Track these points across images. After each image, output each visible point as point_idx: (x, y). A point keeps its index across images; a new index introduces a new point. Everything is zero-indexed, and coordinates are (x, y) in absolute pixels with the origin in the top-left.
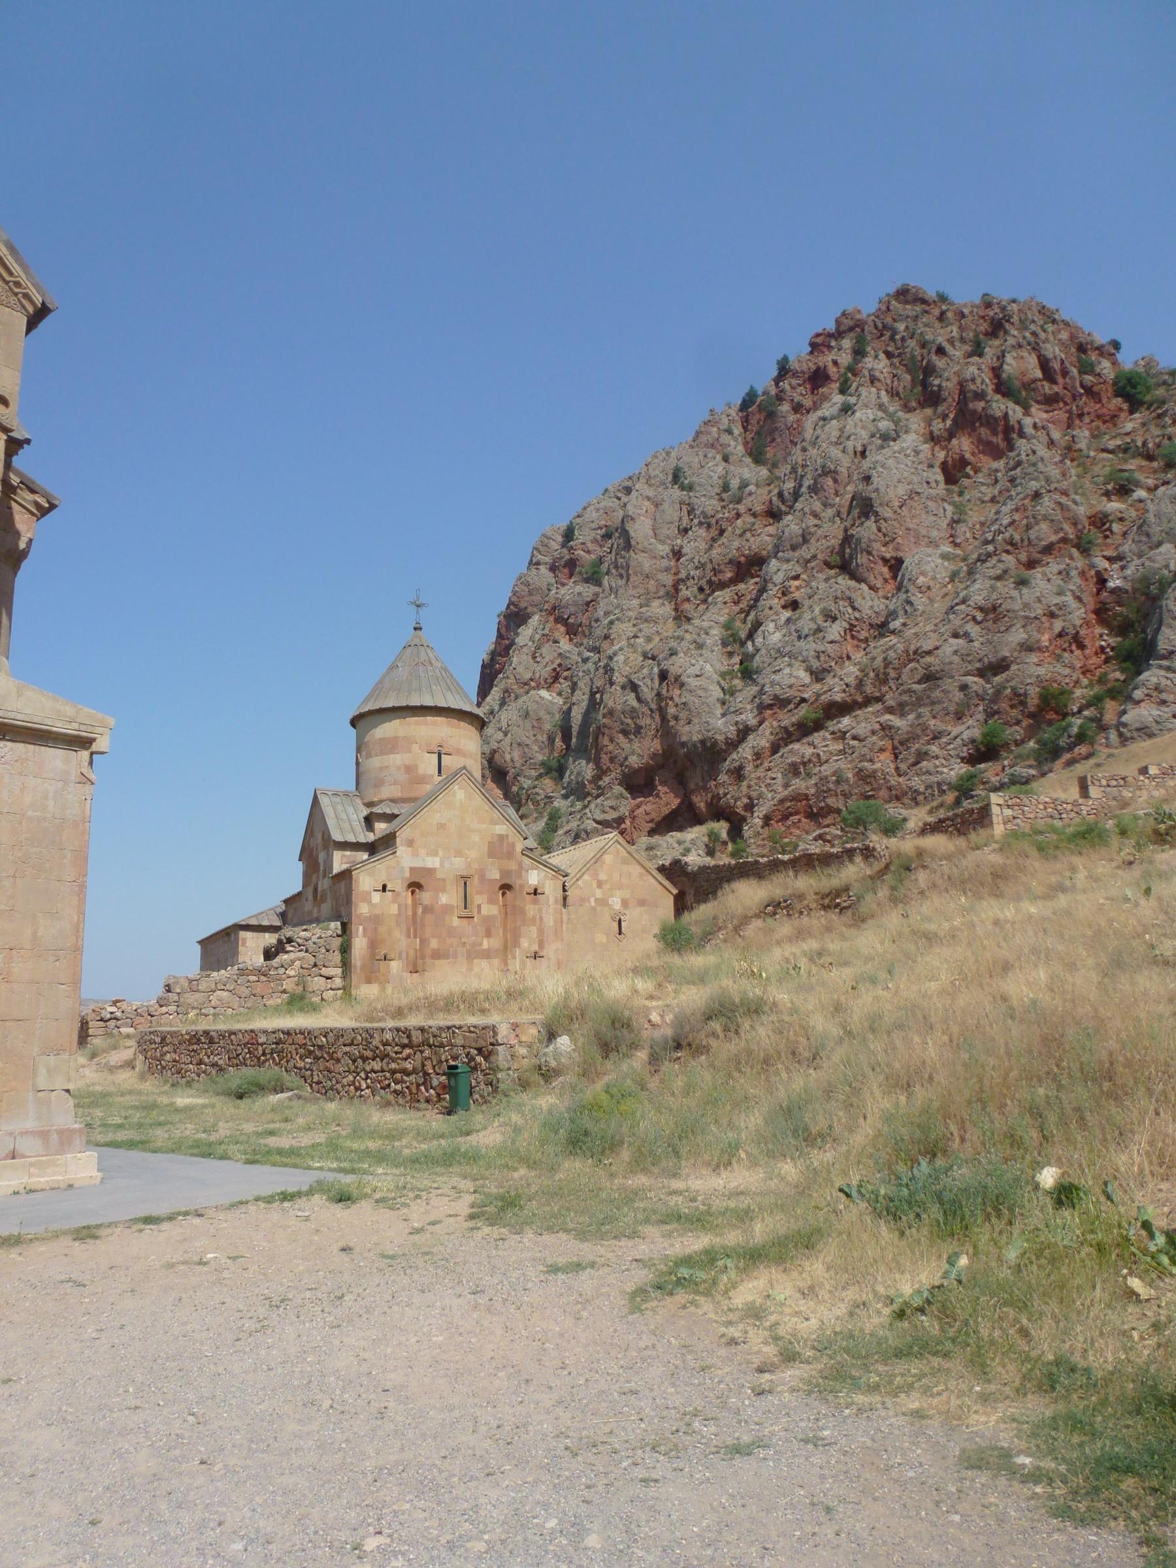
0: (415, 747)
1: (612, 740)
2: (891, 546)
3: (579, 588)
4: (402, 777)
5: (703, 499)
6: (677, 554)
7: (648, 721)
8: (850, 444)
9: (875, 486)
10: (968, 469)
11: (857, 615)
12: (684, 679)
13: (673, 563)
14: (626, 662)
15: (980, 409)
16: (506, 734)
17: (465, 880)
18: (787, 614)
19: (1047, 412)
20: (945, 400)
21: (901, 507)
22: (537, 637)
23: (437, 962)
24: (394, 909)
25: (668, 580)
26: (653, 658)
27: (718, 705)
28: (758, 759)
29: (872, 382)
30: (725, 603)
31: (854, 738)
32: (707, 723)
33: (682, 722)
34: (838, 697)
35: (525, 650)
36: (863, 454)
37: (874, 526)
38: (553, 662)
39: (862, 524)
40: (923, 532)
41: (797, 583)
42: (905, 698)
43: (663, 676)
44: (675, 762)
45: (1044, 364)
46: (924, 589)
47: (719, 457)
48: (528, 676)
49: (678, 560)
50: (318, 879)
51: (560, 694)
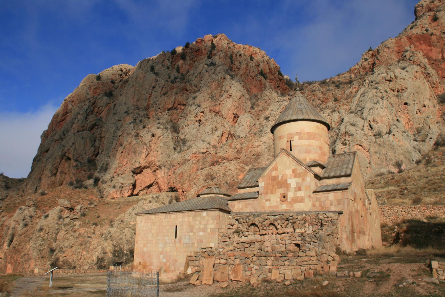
0: (322, 139)
2: (236, 110)
4: (319, 151)
7: (145, 151)
8: (220, 75)
9: (232, 90)
10: (249, 93)
11: (225, 129)
12: (161, 138)
13: (148, 98)
15: (253, 76)
16: (73, 144)
18: (197, 124)
19: (270, 83)
21: (240, 98)
22: (88, 111)
23: (360, 235)
27: (173, 149)
28: (190, 171)
29: (220, 58)
31: (230, 170)
33: (159, 153)
34: (223, 156)
35: (84, 115)
36: (225, 78)
37: (231, 103)
38: (92, 122)
40: (244, 108)
41: (202, 114)
42: (248, 160)
43: (153, 136)
46: (249, 126)
47: (166, 67)
49: (150, 96)
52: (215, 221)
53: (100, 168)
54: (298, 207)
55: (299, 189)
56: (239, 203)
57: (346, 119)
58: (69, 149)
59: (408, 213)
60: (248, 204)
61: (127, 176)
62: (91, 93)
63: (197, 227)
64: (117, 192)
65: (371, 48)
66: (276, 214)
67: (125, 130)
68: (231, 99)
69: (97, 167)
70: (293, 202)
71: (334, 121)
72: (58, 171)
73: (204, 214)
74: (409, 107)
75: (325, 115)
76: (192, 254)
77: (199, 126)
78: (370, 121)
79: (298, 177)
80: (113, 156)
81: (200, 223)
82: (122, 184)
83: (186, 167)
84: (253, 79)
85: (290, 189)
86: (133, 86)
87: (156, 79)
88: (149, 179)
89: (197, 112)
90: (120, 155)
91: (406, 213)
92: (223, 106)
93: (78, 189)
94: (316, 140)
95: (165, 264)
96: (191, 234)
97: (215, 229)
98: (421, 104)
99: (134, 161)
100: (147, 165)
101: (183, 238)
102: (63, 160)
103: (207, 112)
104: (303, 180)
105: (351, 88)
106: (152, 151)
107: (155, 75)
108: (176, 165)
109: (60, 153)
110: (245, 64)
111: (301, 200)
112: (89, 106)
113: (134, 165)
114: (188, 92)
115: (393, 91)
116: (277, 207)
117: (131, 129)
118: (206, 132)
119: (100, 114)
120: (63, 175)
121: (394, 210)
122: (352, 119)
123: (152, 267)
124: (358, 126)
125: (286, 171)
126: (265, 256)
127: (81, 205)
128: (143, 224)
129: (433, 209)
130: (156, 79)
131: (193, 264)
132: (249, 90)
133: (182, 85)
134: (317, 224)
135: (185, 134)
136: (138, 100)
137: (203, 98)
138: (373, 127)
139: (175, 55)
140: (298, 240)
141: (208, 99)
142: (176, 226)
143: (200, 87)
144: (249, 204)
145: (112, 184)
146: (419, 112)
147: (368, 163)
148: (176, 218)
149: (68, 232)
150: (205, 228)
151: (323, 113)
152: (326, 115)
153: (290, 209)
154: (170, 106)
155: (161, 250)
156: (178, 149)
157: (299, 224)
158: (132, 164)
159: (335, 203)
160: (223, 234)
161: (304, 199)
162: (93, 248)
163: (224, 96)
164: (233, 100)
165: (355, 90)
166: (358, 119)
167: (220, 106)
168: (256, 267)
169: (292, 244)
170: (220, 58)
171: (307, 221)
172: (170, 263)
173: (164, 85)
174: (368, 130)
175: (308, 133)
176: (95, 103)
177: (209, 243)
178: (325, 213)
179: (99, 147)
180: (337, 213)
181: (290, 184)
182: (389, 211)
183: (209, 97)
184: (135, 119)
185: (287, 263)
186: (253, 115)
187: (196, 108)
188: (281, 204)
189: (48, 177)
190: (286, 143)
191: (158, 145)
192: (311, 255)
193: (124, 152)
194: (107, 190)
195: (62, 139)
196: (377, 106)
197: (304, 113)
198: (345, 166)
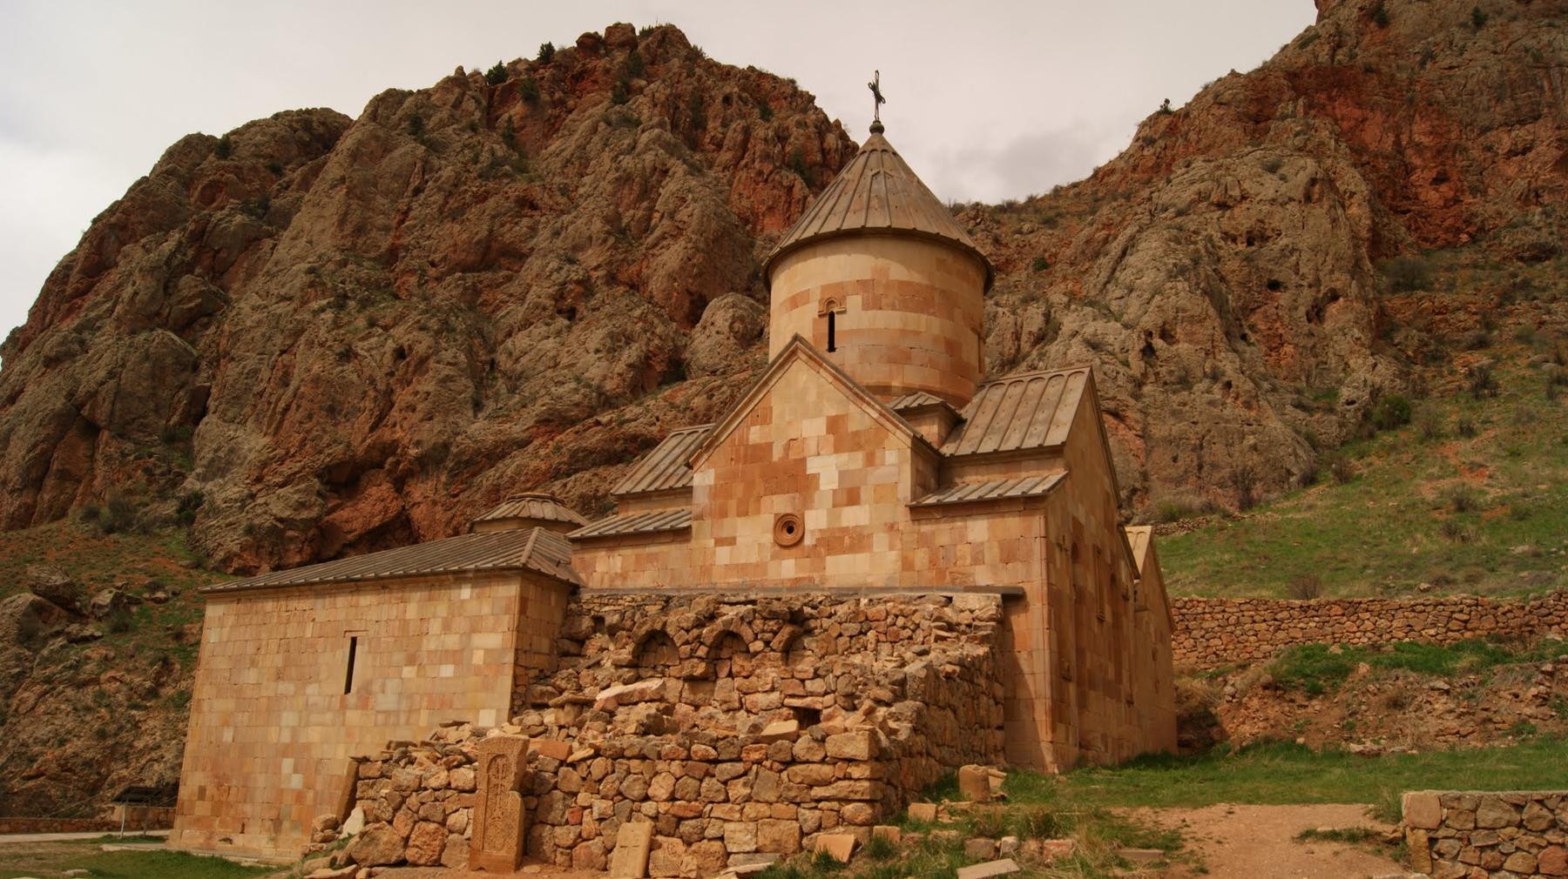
1: (310, 417)
3: (238, 218)
5: (443, 162)
6: (406, 214)
7: (368, 404)
12: (432, 363)
13: (394, 223)
14: (336, 324)
15: (766, 172)
16: (111, 374)
17: (1098, 552)
18: (562, 322)
20: (729, 149)
22: (176, 262)
23: (1092, 694)
24: (1067, 589)
25: (385, 244)
26: (386, 328)
27: (469, 406)
28: (528, 481)
29: (655, 105)
30: (466, 289)
32: (456, 423)
34: (644, 431)
36: (665, 172)
38: (190, 300)
39: (668, 247)
43: (400, 354)
44: (398, 463)
45: (824, 152)
48: (154, 308)
49: (402, 221)
50: (807, 503)
51: (193, 343)
52: (507, 617)
53: (204, 462)
54: (843, 569)
55: (852, 497)
56: (611, 549)
57: (1069, 322)
58: (92, 395)
59: (1278, 629)
60: (649, 555)
61: (297, 492)
62: (192, 200)
63: (432, 646)
64: (258, 547)
65: (1167, 101)
66: (753, 597)
67: (303, 331)
68: (682, 242)
69: (194, 459)
70: (822, 550)
71: (1030, 333)
72: (48, 468)
73: (466, 592)
74: (1283, 298)
75: (1000, 309)
76: (373, 753)
77: (569, 328)
78: (1150, 334)
79: (852, 450)
80: (257, 420)
81: (447, 627)
82: (281, 520)
83: (509, 467)
84: (766, 181)
85: (816, 496)
86: (343, 180)
87: (426, 162)
88: (379, 506)
89: (561, 280)
90: (278, 417)
91: (1271, 629)
92: (653, 265)
93: (115, 536)
94: (933, 314)
95: (299, 797)
96: (409, 672)
97: (504, 650)
98: (1323, 290)
99: (326, 439)
100: (375, 454)
101: (376, 687)
102: (70, 434)
103: (599, 282)
104: (870, 460)
105: (1095, 226)
106: (396, 407)
107: (423, 147)
108: (479, 459)
109: (59, 405)
110: (739, 129)
111: (856, 541)
112: (180, 243)
113: (329, 455)
114: (534, 213)
115: (1234, 240)
116: (760, 567)
117: (323, 329)
118: (591, 351)
119: (222, 274)
120: (67, 484)
121: (1226, 616)
122: (1091, 323)
123: (248, 808)
124: (1110, 348)
125: (806, 423)
126: (643, 758)
127: (115, 591)
128: (226, 630)
129: (1368, 615)
130: (426, 162)
131: (371, 793)
132: (752, 219)
133: (517, 188)
134: (910, 638)
135: (517, 353)
136: (360, 230)
137: (587, 233)
138: (1163, 355)
139: (500, 86)
140: (812, 694)
141: (603, 236)
142: (354, 641)
143: (581, 196)
144: (652, 558)
145: (244, 519)
146: (1317, 314)
147: (1137, 475)
148: (357, 606)
149: (54, 689)
150: (462, 651)
151: (997, 304)
152: (1005, 310)
153: (811, 579)
154: (471, 258)
155: (286, 738)
156: (490, 406)
157: (841, 635)
158: (320, 452)
159: (993, 553)
160: (537, 672)
161: (870, 536)
162: (146, 746)
163: (657, 233)
164: (690, 245)
165: (1103, 234)
166: (1110, 324)
167: (645, 264)
168: (600, 806)
169: (785, 711)
170: (655, 105)
171: (874, 624)
172: (316, 793)
173: (456, 185)
174: (1142, 364)
175: (902, 284)
176: (203, 232)
177: (476, 709)
178: (949, 594)
179: (210, 387)
180: (999, 596)
181: (816, 477)
182: (1207, 616)
183: (609, 233)
184: (345, 297)
185: (738, 790)
186: (758, 301)
187: (561, 268)
188: (774, 557)
189: (12, 492)
190: (815, 320)
191: (419, 388)
192: (849, 751)
193: (294, 406)
194: (221, 541)
195: (71, 356)
196: (1180, 285)
197: (893, 209)
198: (1041, 416)
